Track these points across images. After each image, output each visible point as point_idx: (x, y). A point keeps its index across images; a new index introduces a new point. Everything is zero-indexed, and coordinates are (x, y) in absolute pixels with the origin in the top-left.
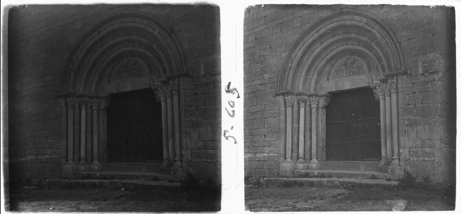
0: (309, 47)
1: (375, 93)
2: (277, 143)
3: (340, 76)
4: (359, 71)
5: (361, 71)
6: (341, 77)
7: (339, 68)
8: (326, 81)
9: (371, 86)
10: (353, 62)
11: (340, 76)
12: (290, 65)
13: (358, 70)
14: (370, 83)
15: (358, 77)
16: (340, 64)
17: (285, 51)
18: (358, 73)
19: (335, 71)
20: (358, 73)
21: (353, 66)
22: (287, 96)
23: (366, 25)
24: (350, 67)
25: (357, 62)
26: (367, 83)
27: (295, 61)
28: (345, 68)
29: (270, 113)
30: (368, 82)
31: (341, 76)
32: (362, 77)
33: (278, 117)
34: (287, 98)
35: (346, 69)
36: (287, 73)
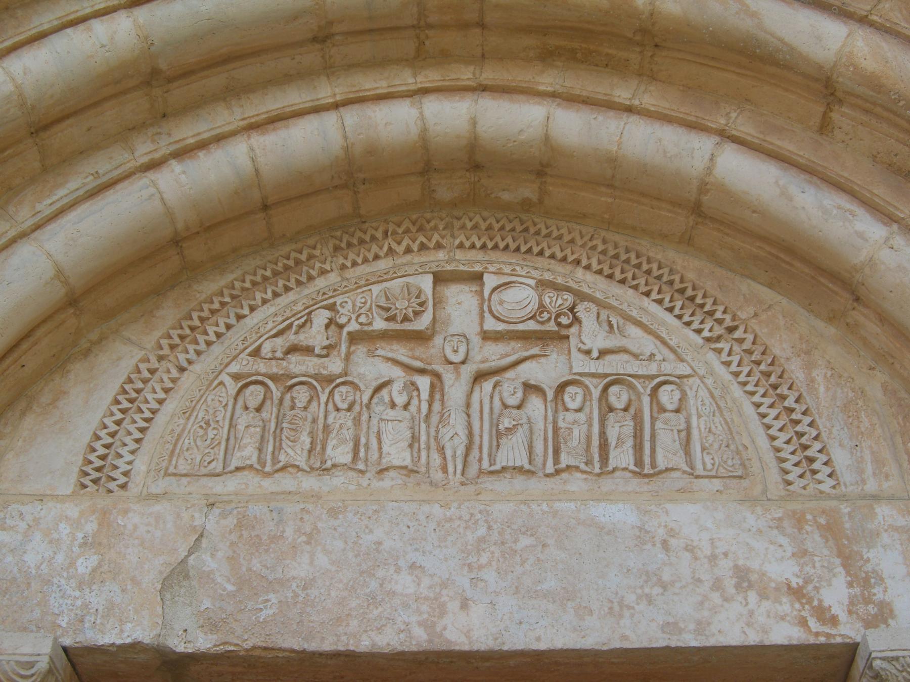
3: (317, 448)
7: (298, 365)
8: (67, 487)
10: (531, 326)
11: (317, 448)
14: (823, 614)
16: (321, 317)
18: (621, 457)
19: (232, 387)
20: (621, 457)
21: (531, 371)
24: (480, 377)
26: (786, 606)
28: (397, 372)
30: (797, 593)
31: (339, 453)
35: (424, 383)
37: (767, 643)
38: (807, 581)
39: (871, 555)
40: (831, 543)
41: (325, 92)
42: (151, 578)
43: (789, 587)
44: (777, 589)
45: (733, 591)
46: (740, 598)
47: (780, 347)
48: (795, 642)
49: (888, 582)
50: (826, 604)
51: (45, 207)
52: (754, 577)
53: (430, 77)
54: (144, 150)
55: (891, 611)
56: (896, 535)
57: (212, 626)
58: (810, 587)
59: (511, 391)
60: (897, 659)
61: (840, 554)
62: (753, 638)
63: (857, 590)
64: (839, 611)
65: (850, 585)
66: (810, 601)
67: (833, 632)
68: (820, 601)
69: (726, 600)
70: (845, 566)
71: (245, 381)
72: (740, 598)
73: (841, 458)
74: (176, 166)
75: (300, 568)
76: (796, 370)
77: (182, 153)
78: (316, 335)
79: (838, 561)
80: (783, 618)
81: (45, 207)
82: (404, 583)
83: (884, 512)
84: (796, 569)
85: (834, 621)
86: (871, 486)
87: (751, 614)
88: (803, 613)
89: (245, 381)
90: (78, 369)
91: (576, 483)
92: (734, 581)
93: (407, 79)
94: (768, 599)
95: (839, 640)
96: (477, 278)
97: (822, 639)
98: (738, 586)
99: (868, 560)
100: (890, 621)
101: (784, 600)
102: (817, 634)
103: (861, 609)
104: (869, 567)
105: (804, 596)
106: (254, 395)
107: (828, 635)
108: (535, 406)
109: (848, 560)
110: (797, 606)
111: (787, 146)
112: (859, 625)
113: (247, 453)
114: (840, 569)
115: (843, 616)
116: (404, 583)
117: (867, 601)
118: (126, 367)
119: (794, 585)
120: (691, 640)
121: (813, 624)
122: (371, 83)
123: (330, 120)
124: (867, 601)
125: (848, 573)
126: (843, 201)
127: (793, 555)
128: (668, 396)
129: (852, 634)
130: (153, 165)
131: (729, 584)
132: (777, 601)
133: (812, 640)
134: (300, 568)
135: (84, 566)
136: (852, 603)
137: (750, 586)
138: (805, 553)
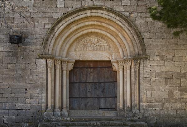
0: (68, 25)
1: (113, 65)
2: (39, 96)
3: (86, 49)
4: (101, 48)
5: (103, 49)
6: (86, 50)
7: (85, 44)
8: (74, 51)
9: (111, 61)
11: (86, 49)
12: (52, 36)
13: (101, 48)
15: (101, 53)
17: (48, 24)
18: (101, 50)
20: (101, 50)
22: (49, 59)
23: (119, 22)
25: (100, 42)
27: (56, 33)
29: (32, 71)
31: (87, 49)
32: (104, 53)
33: (41, 76)
34: (50, 61)
36: (49, 41)
41: (86, 28)
42: (79, 56)
47: (110, 43)
51: (72, 36)
53: (92, 27)
54: (76, 33)
57: (82, 58)
59: (96, 46)
71: (82, 45)
73: (112, 50)
74: (78, 34)
75: (86, 56)
76: (110, 45)
77: (79, 33)
78: (86, 42)
81: (72, 36)
82: (90, 56)
83: (114, 53)
86: (113, 52)
89: (82, 45)
90: (73, 44)
91: (99, 51)
93: (90, 27)
96: (94, 38)
106: (83, 46)
108: (97, 46)
109: (111, 56)
111: (111, 33)
113: (83, 49)
116: (90, 56)
118: (76, 44)
120: (103, 60)
122: (88, 28)
123: (86, 30)
126: (113, 37)
128: (104, 46)
130: (77, 34)
134: (86, 56)
135: (75, 55)
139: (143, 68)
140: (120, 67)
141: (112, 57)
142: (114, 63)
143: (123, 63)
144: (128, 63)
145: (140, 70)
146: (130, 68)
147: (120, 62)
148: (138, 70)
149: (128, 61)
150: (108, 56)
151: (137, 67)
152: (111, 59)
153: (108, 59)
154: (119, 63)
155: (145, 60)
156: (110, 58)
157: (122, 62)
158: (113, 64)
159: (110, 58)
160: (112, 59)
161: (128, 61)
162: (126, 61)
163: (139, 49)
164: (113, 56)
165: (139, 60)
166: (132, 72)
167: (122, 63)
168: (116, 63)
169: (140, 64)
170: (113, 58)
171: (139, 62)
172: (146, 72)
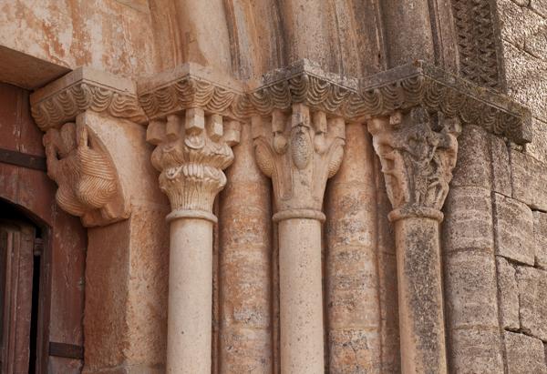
14: (57, 46)
26: (40, 35)
30: (47, 30)
37: (26, 53)
38: (54, 25)
39: (87, 23)
40: (69, 8)
43: (44, 25)
44: (37, 24)
45: (14, 16)
46: (17, 21)
48: (40, 58)
49: (93, 42)
50: (60, 42)
52: (27, 12)
55: (90, 58)
56: (102, 18)
58: (54, 29)
60: (94, 87)
61: (72, 16)
62: (19, 48)
63: (76, 40)
64: (66, 48)
65: (74, 36)
66: (53, 37)
67: (61, 59)
68: (57, 39)
69: (9, 19)
70: (73, 24)
72: (17, 21)
79: (71, 20)
80: (37, 42)
84: (49, 16)
85: (62, 53)
87: (21, 33)
88: (49, 43)
92: (16, 10)
94: (31, 27)
95: (62, 64)
97: (54, 61)
98: (17, 14)
99: (85, 25)
100: (89, 64)
101: (40, 31)
102: (52, 57)
103: (77, 51)
104: (84, 29)
105: (50, 33)
107: (57, 60)
109: (76, 21)
110: (46, 37)
112: (74, 60)
114: (71, 25)
115: (67, 52)
117: (80, 48)
119: (46, 24)
121: (51, 50)
124: (80, 48)
125: (74, 29)
127: (49, 7)
129: (69, 64)
131: (13, 11)
132: (36, 30)
133: (49, 60)
136: (72, 46)
137: (24, 17)
138: (55, 8)
139: (490, 222)
140: (195, 170)
141: (81, 36)
142: (106, 113)
143: (233, 136)
144: (320, 141)
145: (458, 240)
146: (320, 205)
147: (208, 117)
148: (436, 226)
149: (322, 119)
150: (42, 14)
151: (436, 199)
152: (68, 61)
153: (36, 51)
154: (198, 120)
155: (500, 143)
156: (66, 38)
157: (226, 120)
158: (92, 120)
159: (66, 38)
160: (85, 59)
161: (322, 119)
162: (302, 114)
163: (440, 17)
164: (95, 28)
165: (458, 128)
166: (337, 248)
167: (218, 128)
168: (124, 116)
169: (454, 172)
170: (97, 49)
171: (454, 143)
172: (511, 267)
